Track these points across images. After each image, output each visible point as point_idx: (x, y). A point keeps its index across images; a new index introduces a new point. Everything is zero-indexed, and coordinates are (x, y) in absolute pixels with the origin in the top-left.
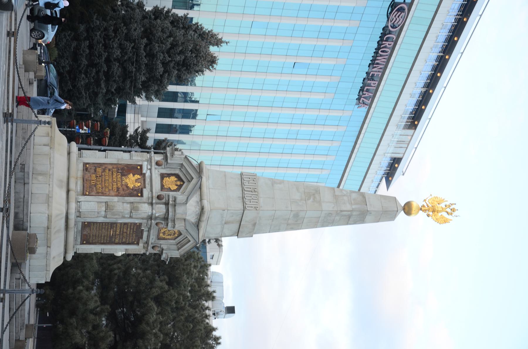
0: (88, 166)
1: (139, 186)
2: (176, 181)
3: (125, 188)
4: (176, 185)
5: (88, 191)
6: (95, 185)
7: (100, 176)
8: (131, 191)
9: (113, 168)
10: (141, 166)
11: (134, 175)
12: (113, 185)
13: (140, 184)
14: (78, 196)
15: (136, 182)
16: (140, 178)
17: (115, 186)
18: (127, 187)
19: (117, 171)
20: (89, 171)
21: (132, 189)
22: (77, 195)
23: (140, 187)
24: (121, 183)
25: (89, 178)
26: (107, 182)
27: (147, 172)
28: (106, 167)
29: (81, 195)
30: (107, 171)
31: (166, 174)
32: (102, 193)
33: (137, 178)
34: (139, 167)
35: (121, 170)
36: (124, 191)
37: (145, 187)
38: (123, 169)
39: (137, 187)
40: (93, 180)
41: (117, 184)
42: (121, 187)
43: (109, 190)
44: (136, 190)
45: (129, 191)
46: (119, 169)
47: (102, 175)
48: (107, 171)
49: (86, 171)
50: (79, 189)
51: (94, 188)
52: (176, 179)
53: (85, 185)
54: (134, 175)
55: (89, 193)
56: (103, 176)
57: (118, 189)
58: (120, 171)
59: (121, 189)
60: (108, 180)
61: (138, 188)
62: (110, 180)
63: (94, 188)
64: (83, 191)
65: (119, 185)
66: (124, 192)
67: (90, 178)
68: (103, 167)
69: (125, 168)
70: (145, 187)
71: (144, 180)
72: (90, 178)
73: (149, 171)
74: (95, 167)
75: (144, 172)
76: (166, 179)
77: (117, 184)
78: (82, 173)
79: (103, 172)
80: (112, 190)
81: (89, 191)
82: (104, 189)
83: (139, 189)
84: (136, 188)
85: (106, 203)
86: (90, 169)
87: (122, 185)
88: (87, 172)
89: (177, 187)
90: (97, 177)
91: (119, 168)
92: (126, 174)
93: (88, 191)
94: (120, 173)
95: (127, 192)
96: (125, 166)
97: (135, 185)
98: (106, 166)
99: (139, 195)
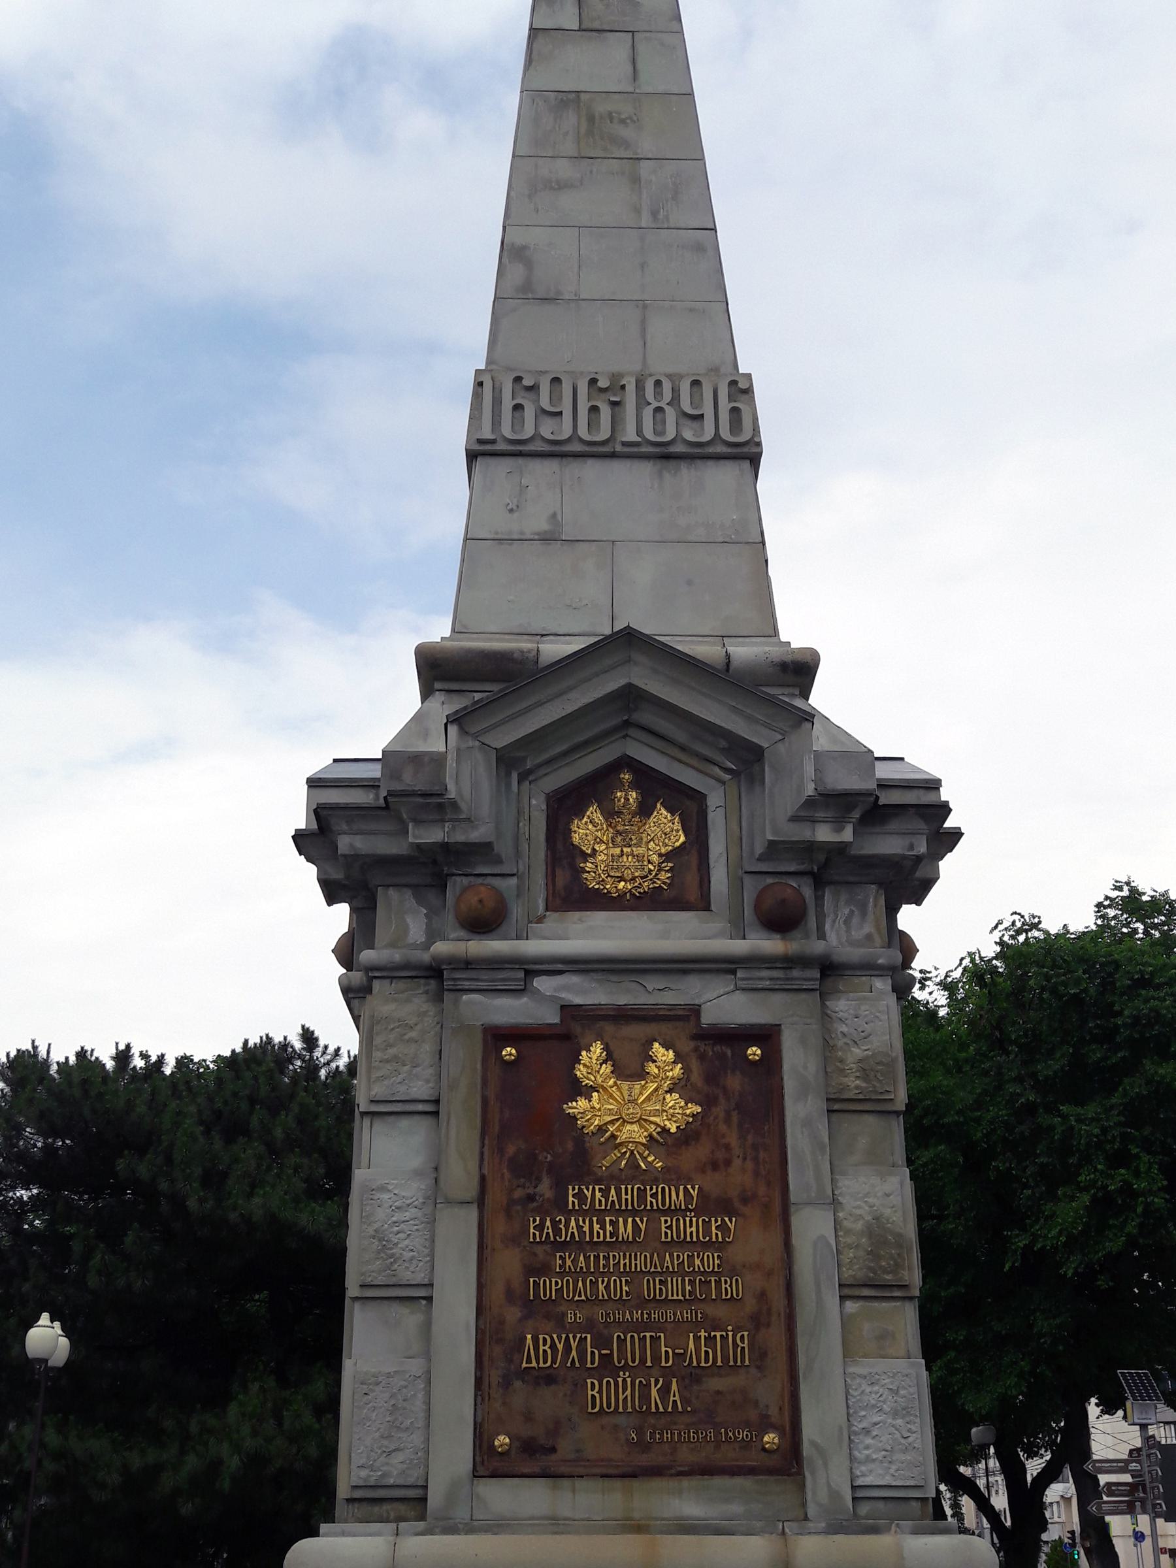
0: (502, 1440)
1: (678, 1058)
2: (610, 814)
3: (702, 1151)
4: (645, 810)
5: (744, 1434)
6: (692, 1377)
7: (602, 1341)
8: (719, 1111)
9: (517, 1238)
10: (498, 1036)
11: (578, 1090)
12: (682, 1244)
13: (656, 1045)
14: (812, 1510)
15: (642, 1075)
16: (606, 1048)
17: (692, 1228)
18: (688, 1136)
19: (543, 1212)
20: (556, 1428)
21: (708, 1103)
22: (806, 1518)
23: (687, 1046)
24: (656, 1181)
25: (616, 1427)
26: (651, 1288)
27: (553, 999)
28: (510, 1296)
29: (802, 1487)
30: (550, 1286)
31: (551, 875)
32: (758, 1322)
33: (606, 1069)
34: (509, 1052)
35: (539, 1180)
36: (728, 1163)
37: (695, 1011)
38: (524, 1168)
39: (686, 1070)
40: (645, 1397)
41: (668, 1212)
42: (689, 1180)
43: (730, 1270)
44: (711, 1078)
45: (723, 1127)
46: (531, 1198)
47: (590, 1325)
48: (550, 1286)
49: (553, 1450)
50: (736, 1508)
51: (715, 1384)
52: (594, 812)
53: (686, 1456)
54: (578, 1090)
55: (766, 1425)
56: (600, 1313)
57: (709, 1205)
58: (545, 1189)
59: (712, 1182)
60: (633, 1276)
61: (695, 1064)
62: (639, 1263)
63: (715, 1384)
64: (751, 1471)
65: (676, 1197)
66: (737, 1162)
67: (621, 1420)
68: (513, 1314)
69: (511, 1150)
70: (695, 1011)
71: (623, 1015)
72: (621, 1420)
73: (542, 984)
74: (506, 1383)
75: (551, 1017)
76: (594, 874)
77: (668, 1212)
78: (579, 1483)
79: (560, 1322)
80: (720, 1246)
81: (747, 1424)
82: (719, 1312)
83: (702, 1057)
84: (696, 1077)
85: (847, 1291)
86: (529, 1417)
87: (673, 1176)
88: (565, 1447)
89: (662, 814)
90: (607, 1367)
91: (519, 1193)
92: (570, 1146)
93: (744, 1434)
94: (560, 1188)
95: (733, 1139)
96: (501, 1151)
97: (666, 1086)
98: (497, 1293)
99: (754, 1052)
